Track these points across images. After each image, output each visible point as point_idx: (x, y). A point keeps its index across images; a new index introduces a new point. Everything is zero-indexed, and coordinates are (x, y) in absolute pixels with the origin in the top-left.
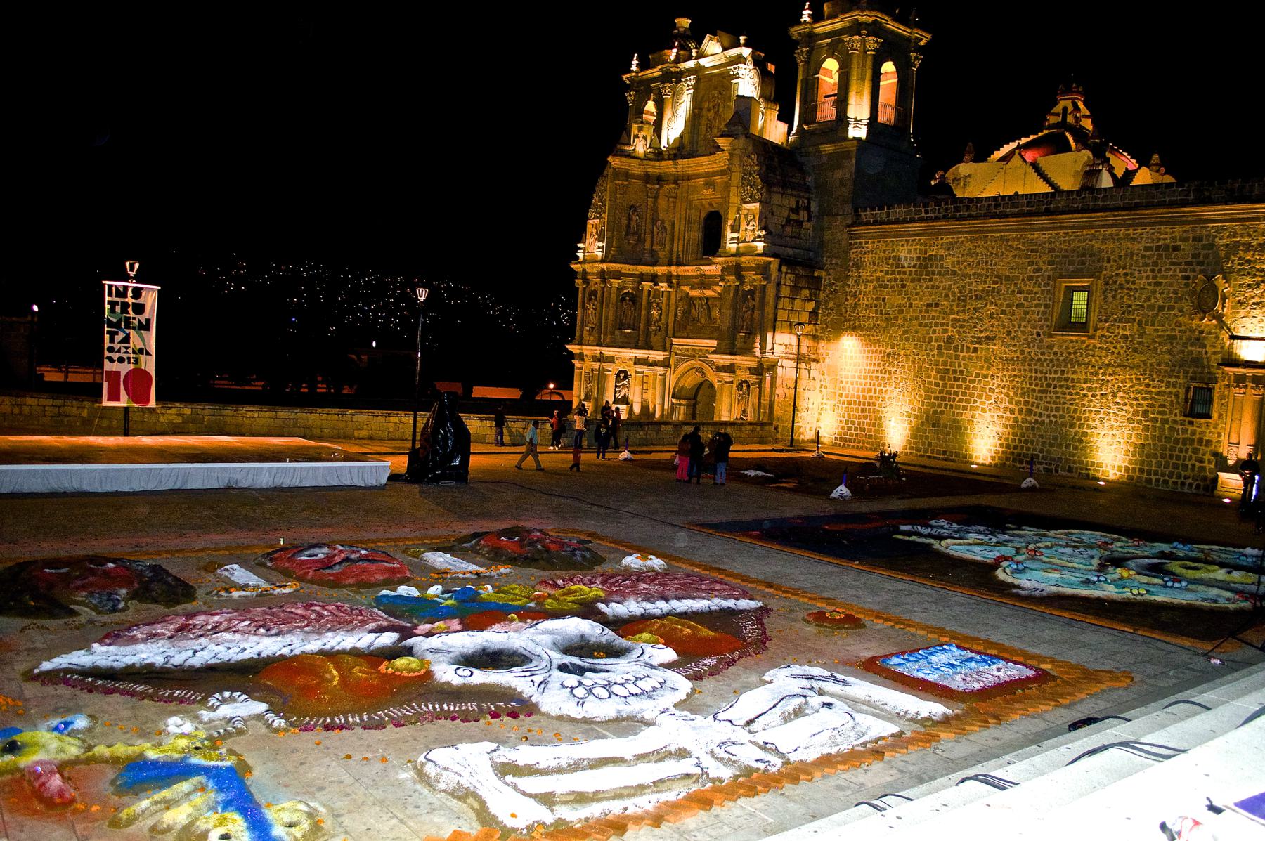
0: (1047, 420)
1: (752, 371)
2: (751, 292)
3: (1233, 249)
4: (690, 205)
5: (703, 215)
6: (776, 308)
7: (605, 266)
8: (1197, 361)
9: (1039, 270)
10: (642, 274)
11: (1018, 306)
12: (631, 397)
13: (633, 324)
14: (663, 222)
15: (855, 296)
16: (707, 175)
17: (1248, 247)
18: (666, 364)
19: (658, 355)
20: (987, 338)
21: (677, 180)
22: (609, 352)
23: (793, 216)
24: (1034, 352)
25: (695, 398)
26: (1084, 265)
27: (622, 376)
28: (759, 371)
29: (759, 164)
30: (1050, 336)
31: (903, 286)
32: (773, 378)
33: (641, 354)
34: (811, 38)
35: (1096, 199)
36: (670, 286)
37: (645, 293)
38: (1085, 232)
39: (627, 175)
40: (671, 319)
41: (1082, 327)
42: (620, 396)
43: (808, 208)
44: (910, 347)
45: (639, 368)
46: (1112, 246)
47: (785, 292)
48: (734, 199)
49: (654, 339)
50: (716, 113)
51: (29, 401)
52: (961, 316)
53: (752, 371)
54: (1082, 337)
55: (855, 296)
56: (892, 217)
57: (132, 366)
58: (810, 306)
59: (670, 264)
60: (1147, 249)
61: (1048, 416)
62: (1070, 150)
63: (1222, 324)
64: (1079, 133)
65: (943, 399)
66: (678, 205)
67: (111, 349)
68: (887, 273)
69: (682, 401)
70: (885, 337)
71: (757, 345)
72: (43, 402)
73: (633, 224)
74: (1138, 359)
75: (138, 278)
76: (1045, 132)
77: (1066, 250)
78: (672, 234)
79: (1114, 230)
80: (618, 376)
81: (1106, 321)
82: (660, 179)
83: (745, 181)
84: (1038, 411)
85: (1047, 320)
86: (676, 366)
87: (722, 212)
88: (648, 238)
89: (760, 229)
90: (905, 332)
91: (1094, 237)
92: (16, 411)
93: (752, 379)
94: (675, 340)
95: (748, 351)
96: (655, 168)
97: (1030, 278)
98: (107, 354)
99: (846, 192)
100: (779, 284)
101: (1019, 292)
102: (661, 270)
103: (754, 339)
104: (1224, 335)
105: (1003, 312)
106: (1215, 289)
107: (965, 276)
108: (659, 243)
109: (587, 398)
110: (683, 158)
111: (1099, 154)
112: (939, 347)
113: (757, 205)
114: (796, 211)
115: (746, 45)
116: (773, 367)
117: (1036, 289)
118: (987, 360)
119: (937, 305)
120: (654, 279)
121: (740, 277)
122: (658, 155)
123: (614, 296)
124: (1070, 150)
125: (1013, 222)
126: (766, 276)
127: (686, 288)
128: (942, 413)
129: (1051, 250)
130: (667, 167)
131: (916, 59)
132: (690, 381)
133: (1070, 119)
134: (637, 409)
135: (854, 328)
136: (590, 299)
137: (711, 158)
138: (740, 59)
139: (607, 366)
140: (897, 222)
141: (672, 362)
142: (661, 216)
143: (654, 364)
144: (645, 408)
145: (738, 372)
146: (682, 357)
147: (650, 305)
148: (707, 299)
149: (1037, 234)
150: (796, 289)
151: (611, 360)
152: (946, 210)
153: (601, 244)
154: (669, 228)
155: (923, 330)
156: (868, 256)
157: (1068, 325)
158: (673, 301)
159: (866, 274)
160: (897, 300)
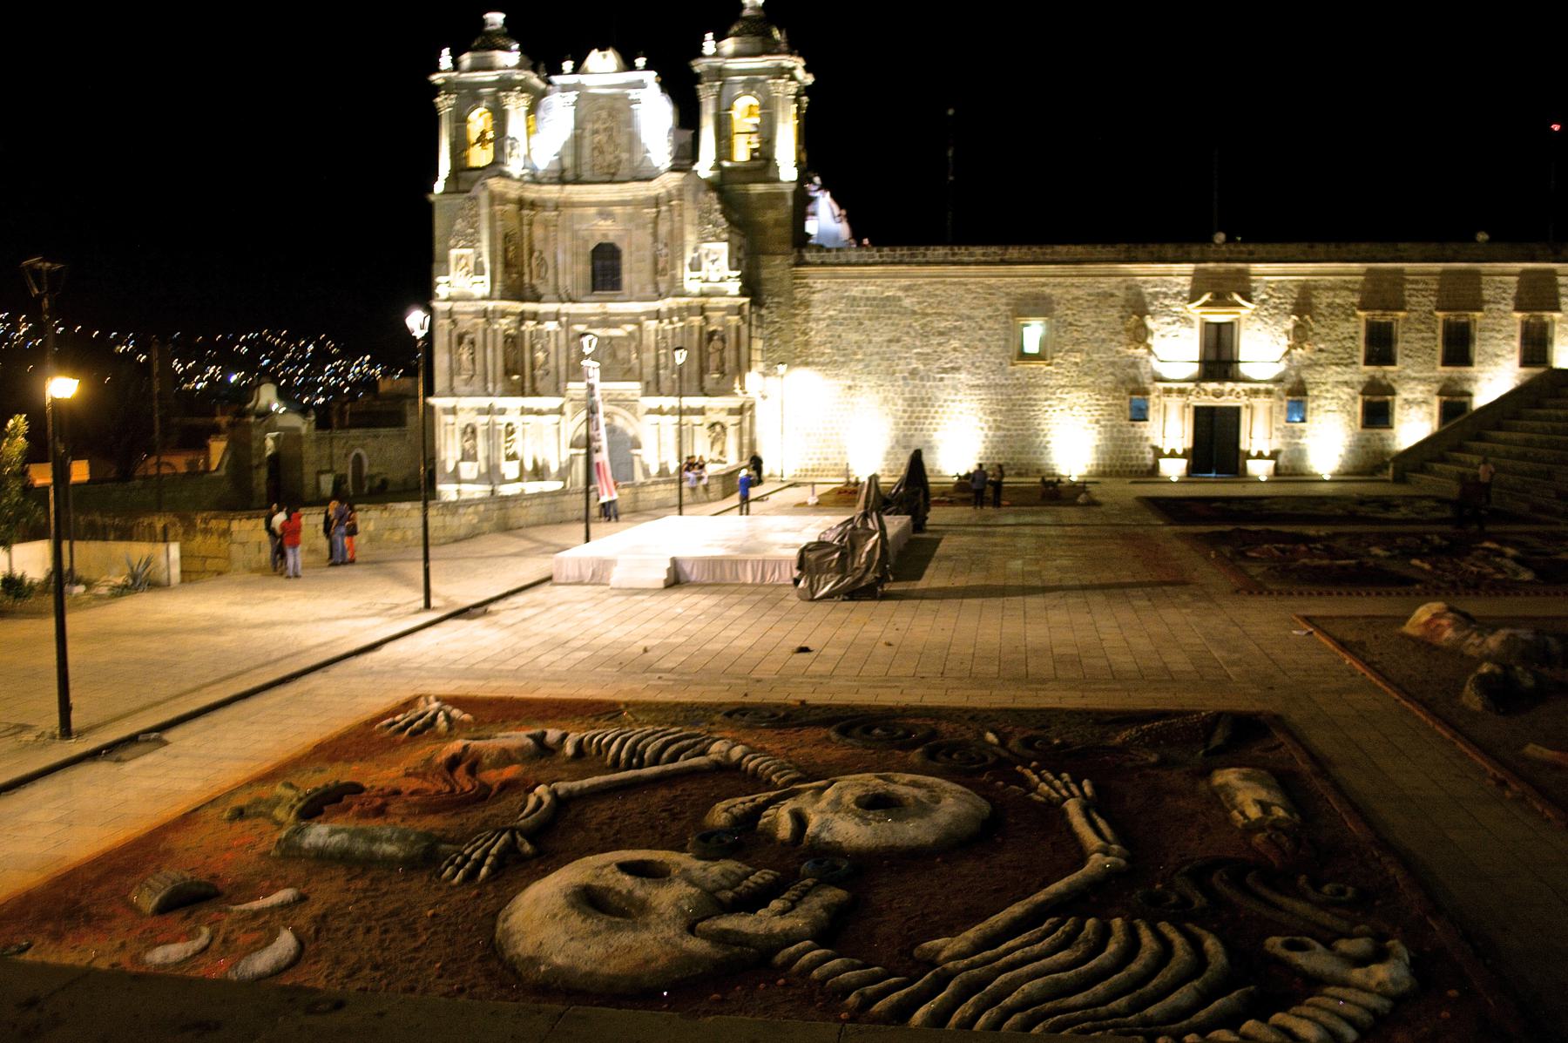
1: (731, 412)
2: (713, 333)
3: (1155, 296)
4: (575, 235)
5: (592, 246)
7: (490, 305)
8: (1135, 380)
10: (522, 313)
11: (981, 340)
13: (518, 371)
15: (805, 333)
17: (1166, 295)
18: (560, 411)
21: (557, 206)
22: (499, 402)
24: (999, 379)
26: (1038, 305)
28: (740, 411)
32: (752, 417)
34: (720, 74)
36: (560, 324)
37: (527, 336)
40: (562, 362)
42: (511, 451)
44: (873, 380)
48: (691, 238)
49: (539, 385)
50: (610, 137)
52: (926, 350)
53: (731, 412)
54: (1041, 365)
55: (805, 333)
63: (1151, 352)
66: (560, 235)
70: (845, 371)
71: (737, 385)
73: (510, 255)
74: (1088, 380)
78: (556, 267)
82: (533, 205)
83: (703, 219)
87: (619, 245)
88: (526, 270)
90: (867, 366)
91: (1044, 285)
94: (571, 385)
95: (728, 392)
96: (532, 193)
104: (1152, 359)
106: (1144, 326)
107: (927, 315)
108: (538, 276)
109: (468, 456)
112: (904, 378)
115: (647, 67)
116: (752, 407)
118: (954, 387)
119: (898, 341)
120: (535, 316)
121: (706, 319)
122: (536, 180)
123: (500, 339)
125: (972, 269)
129: (1008, 294)
134: (529, 467)
135: (807, 364)
138: (640, 85)
139: (499, 419)
140: (848, 264)
141: (568, 408)
142: (537, 246)
143: (539, 413)
144: (535, 463)
145: (709, 414)
147: (532, 347)
148: (611, 338)
149: (993, 280)
151: (502, 412)
153: (479, 278)
154: (550, 263)
155: (885, 364)
156: (816, 297)
157: (1023, 356)
158: (562, 340)
159: (816, 312)
160: (854, 337)
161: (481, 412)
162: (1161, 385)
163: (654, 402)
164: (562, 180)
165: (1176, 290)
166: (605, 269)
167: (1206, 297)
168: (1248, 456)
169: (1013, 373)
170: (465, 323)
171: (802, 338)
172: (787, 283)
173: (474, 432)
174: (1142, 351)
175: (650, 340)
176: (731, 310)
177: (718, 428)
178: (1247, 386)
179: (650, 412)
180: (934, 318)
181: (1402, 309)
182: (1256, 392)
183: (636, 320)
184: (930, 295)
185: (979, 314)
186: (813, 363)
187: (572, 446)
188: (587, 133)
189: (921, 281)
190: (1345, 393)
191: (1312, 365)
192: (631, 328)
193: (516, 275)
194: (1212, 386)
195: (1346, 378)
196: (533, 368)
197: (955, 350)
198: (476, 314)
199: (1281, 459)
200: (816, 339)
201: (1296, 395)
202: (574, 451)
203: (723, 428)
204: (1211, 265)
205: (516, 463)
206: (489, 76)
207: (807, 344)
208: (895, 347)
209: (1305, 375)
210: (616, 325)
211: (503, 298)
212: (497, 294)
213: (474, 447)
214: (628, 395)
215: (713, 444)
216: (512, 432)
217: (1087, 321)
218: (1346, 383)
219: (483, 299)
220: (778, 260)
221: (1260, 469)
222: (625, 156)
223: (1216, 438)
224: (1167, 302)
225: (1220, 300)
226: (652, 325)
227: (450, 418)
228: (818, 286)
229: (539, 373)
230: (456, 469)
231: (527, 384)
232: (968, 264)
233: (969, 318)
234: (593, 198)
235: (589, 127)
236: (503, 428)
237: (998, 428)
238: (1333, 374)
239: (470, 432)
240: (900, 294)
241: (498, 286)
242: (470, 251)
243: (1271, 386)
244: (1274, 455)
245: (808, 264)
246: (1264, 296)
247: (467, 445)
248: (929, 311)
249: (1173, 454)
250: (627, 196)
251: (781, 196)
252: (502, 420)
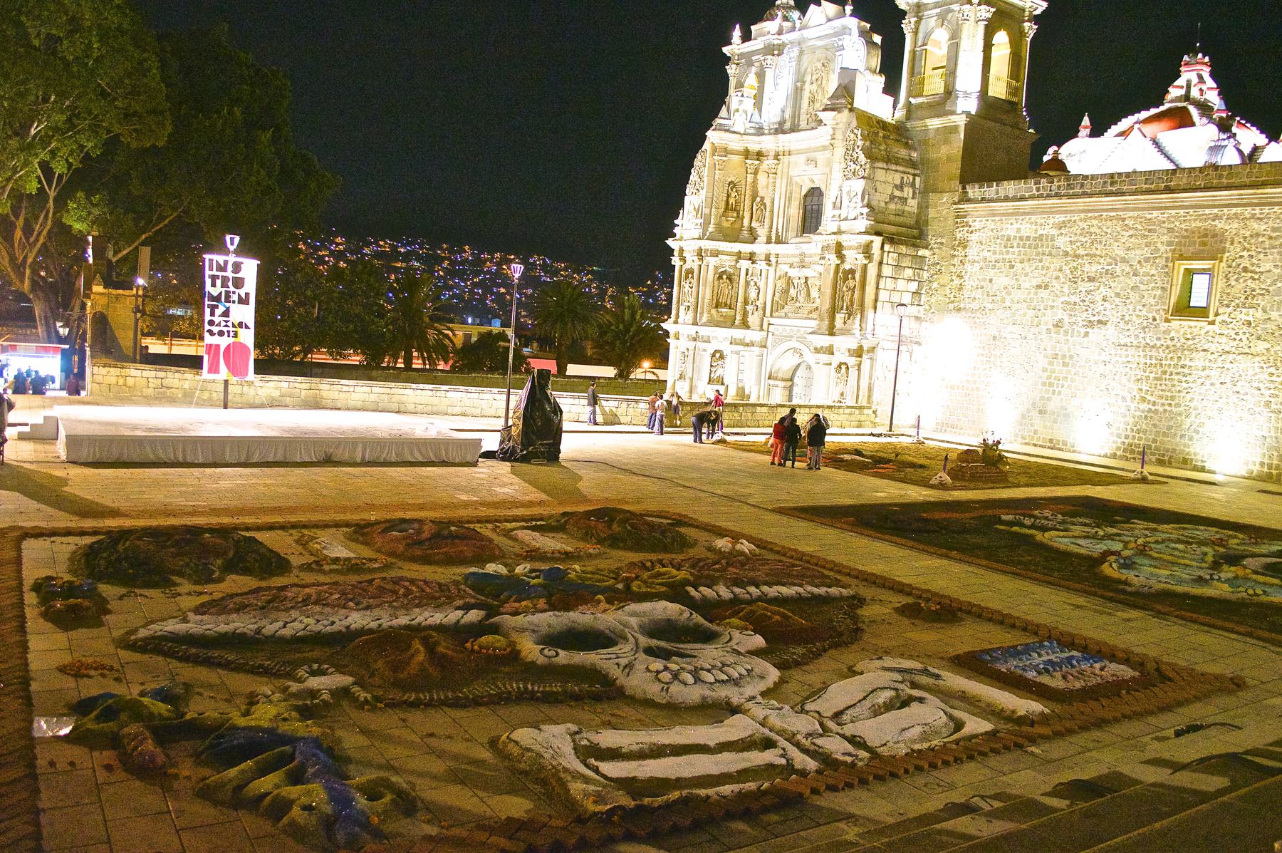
0: (1161, 409)
2: (852, 272)
4: (790, 179)
9: (1157, 250)
14: (762, 198)
20: (1100, 322)
22: (704, 331)
23: (897, 193)
25: (791, 380)
26: (1207, 246)
27: (718, 356)
28: (859, 353)
29: (864, 138)
30: (1167, 320)
35: (1220, 177)
38: (1207, 211)
39: (727, 152)
41: (1202, 312)
43: (913, 185)
46: (1236, 225)
47: (887, 271)
49: (753, 319)
51: (133, 372)
52: (1073, 299)
56: (1002, 195)
57: (231, 340)
58: (913, 286)
60: (1274, 229)
61: (1163, 405)
62: (1193, 124)
64: (1205, 108)
65: (1051, 385)
66: (778, 181)
67: (211, 323)
68: (995, 253)
69: (781, 384)
72: (146, 374)
73: (732, 201)
74: (1262, 346)
75: (238, 252)
76: (1167, 106)
77: (1186, 230)
78: (772, 211)
79: (1239, 210)
80: (713, 356)
81: (1228, 306)
82: (759, 155)
84: (1152, 399)
85: (1164, 303)
87: (823, 189)
91: (1216, 217)
92: (121, 381)
93: (852, 361)
94: (772, 320)
96: (755, 144)
97: (1147, 260)
98: (207, 327)
99: (956, 168)
101: (1135, 275)
105: (1118, 295)
107: (1078, 256)
111: (1224, 127)
114: (900, 187)
116: (872, 350)
117: (1153, 272)
119: (1046, 287)
120: (752, 257)
124: (1193, 124)
128: (1049, 399)
129: (1170, 230)
130: (768, 143)
131: (1030, 29)
133: (1195, 93)
136: (687, 277)
138: (845, 30)
140: (1006, 199)
141: (769, 344)
146: (781, 339)
149: (1156, 213)
150: (898, 267)
152: (1059, 187)
154: (768, 205)
155: (1031, 313)
156: (974, 237)
159: (972, 252)
164: (780, 130)
169: (1167, 332)
171: (957, 281)
172: (950, 222)
177: (843, 367)
180: (1086, 260)
184: (1085, 232)
185: (1135, 255)
188: (807, 84)
189: (1076, 217)
193: (733, 222)
196: (746, 302)
200: (968, 284)
208: (1043, 293)
217: (1267, 266)
220: (945, 197)
228: (977, 225)
229: (749, 308)
231: (738, 318)
232: (1123, 194)
233: (1124, 260)
240: (1054, 232)
241: (711, 229)
245: (969, 201)
248: (1081, 252)
251: (954, 129)
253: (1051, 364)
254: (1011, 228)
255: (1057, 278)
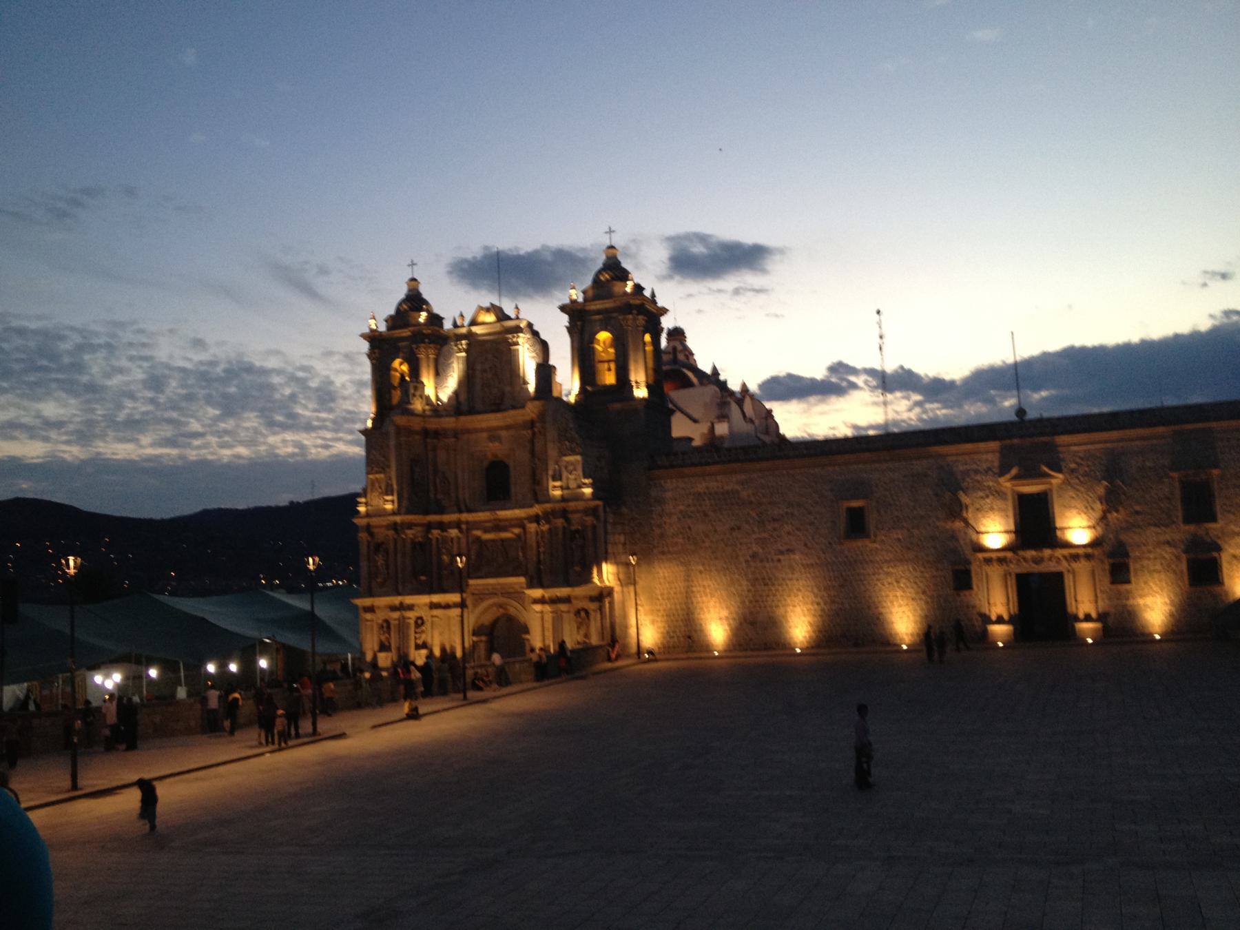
1: (592, 599)
2: (577, 531)
3: (966, 473)
5: (486, 463)
6: (606, 543)
7: (398, 519)
11: (812, 524)
12: (429, 641)
15: (660, 526)
16: (488, 430)
17: (976, 472)
18: (462, 605)
19: (455, 598)
20: (788, 550)
21: (456, 434)
22: (409, 600)
27: (420, 622)
30: (841, 543)
31: (706, 515)
32: (611, 603)
33: (436, 598)
37: (434, 542)
39: (409, 431)
42: (420, 642)
45: (436, 612)
47: (609, 528)
48: (552, 452)
52: (765, 535)
53: (592, 599)
54: (867, 542)
59: (460, 512)
69: (483, 638)
80: (416, 622)
82: (437, 434)
86: (475, 606)
89: (585, 477)
93: (592, 606)
94: (471, 582)
96: (433, 424)
100: (606, 522)
102: (447, 518)
103: (591, 573)
104: (970, 532)
105: (799, 529)
109: (384, 647)
110: (465, 414)
112: (747, 561)
113: (579, 458)
119: (739, 528)
120: (442, 526)
121: (567, 520)
126: (597, 517)
127: (478, 533)
130: (449, 423)
132: (487, 619)
134: (437, 652)
137: (499, 415)
140: (694, 465)
141: (469, 602)
143: (447, 606)
144: (443, 650)
145: (574, 601)
146: (480, 596)
147: (439, 553)
148: (502, 540)
151: (411, 608)
156: (669, 495)
161: (393, 608)
162: (981, 556)
163: (537, 593)
165: (985, 466)
166: (497, 484)
167: (1014, 471)
168: (1076, 619)
170: (381, 534)
171: (658, 531)
173: (389, 627)
174: (959, 525)
175: (532, 540)
176: (586, 512)
178: (1066, 552)
179: (536, 601)
181: (1216, 466)
182: (1075, 557)
183: (520, 523)
186: (669, 552)
187: (474, 634)
190: (1167, 552)
191: (1130, 527)
192: (517, 531)
194: (1030, 553)
195: (1168, 537)
197: (789, 533)
198: (388, 527)
199: (1110, 621)
201: (1114, 560)
202: (475, 639)
203: (587, 612)
204: (1016, 441)
205: (424, 652)
206: (406, 333)
207: (662, 536)
209: (1123, 537)
210: (505, 529)
211: (408, 512)
212: (403, 510)
213: (388, 640)
214: (517, 587)
215: (578, 628)
216: (423, 623)
218: (1168, 543)
219: (394, 513)
221: (1087, 629)
222: (508, 389)
223: (1041, 602)
224: (978, 477)
225: (1029, 473)
226: (532, 527)
227: (368, 616)
230: (375, 657)
234: (484, 425)
235: (478, 367)
236: (412, 622)
237: (833, 602)
238: (1152, 534)
239: (386, 626)
240: (738, 487)
241: (405, 503)
242: (382, 476)
243: (1090, 550)
244: (1102, 617)
245: (660, 467)
246: (1073, 466)
247: (383, 638)
249: (1000, 620)
250: (509, 421)
252: (412, 615)
253: (753, 585)
254: (701, 487)
255: (747, 522)
